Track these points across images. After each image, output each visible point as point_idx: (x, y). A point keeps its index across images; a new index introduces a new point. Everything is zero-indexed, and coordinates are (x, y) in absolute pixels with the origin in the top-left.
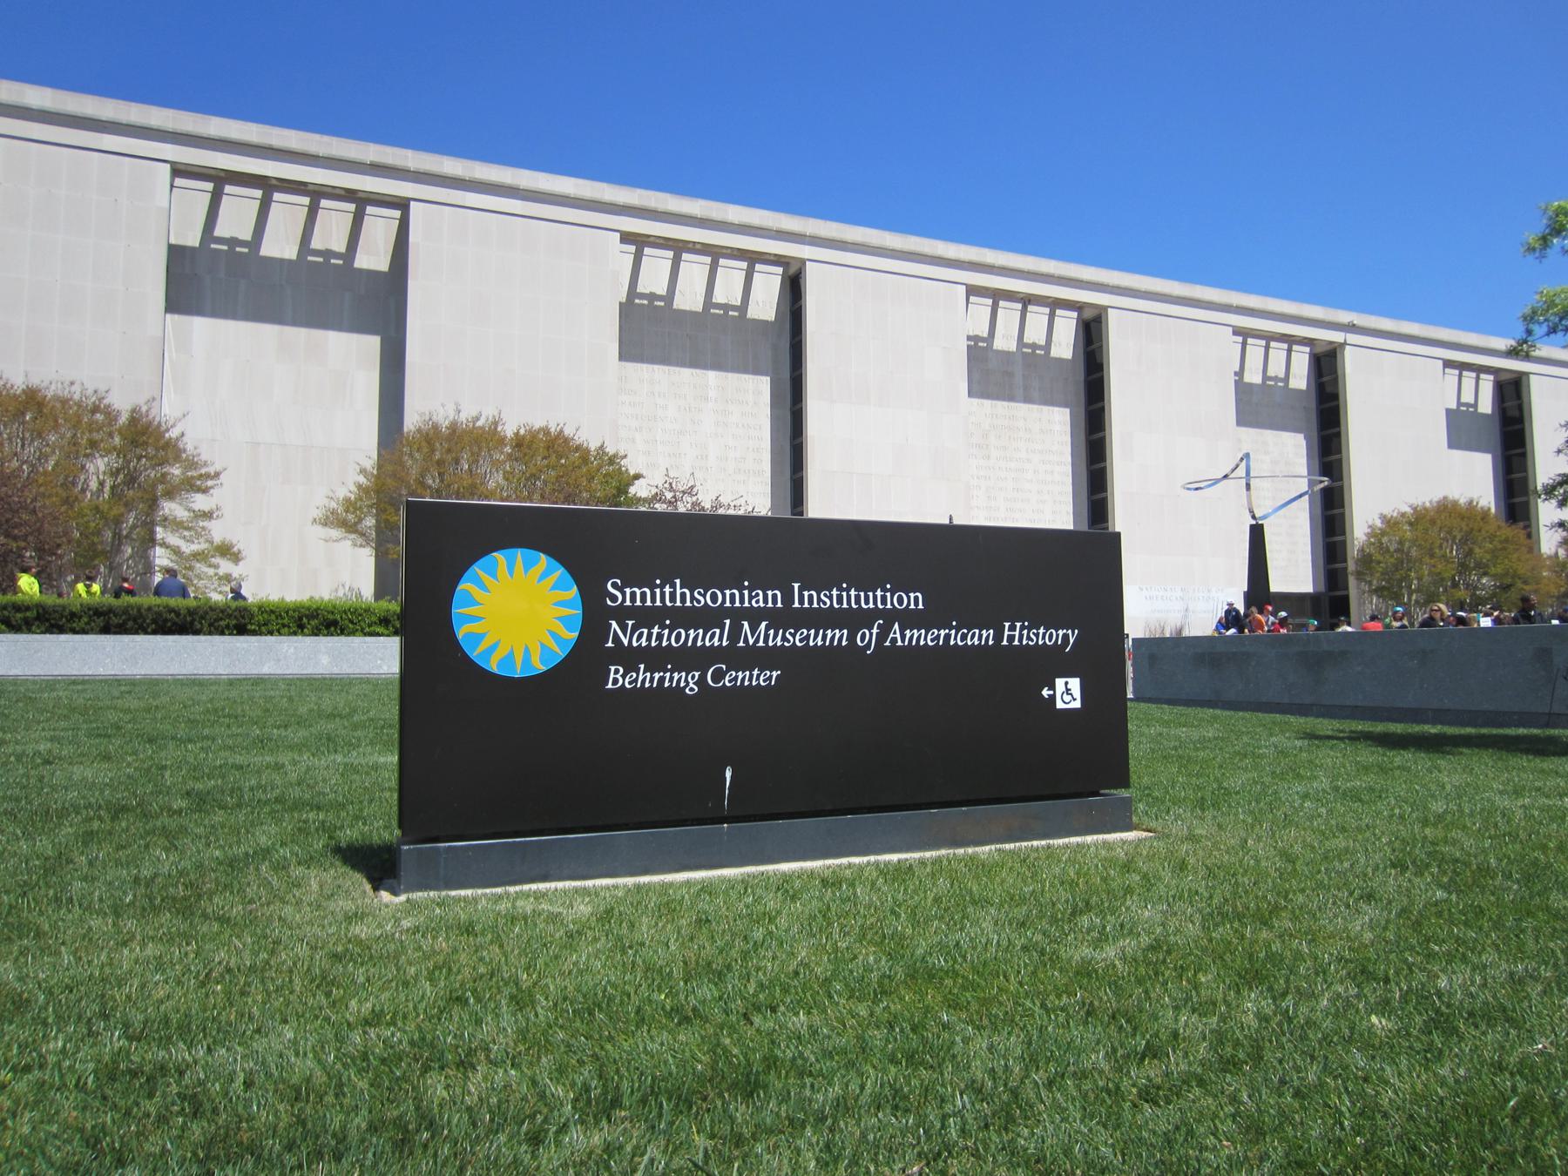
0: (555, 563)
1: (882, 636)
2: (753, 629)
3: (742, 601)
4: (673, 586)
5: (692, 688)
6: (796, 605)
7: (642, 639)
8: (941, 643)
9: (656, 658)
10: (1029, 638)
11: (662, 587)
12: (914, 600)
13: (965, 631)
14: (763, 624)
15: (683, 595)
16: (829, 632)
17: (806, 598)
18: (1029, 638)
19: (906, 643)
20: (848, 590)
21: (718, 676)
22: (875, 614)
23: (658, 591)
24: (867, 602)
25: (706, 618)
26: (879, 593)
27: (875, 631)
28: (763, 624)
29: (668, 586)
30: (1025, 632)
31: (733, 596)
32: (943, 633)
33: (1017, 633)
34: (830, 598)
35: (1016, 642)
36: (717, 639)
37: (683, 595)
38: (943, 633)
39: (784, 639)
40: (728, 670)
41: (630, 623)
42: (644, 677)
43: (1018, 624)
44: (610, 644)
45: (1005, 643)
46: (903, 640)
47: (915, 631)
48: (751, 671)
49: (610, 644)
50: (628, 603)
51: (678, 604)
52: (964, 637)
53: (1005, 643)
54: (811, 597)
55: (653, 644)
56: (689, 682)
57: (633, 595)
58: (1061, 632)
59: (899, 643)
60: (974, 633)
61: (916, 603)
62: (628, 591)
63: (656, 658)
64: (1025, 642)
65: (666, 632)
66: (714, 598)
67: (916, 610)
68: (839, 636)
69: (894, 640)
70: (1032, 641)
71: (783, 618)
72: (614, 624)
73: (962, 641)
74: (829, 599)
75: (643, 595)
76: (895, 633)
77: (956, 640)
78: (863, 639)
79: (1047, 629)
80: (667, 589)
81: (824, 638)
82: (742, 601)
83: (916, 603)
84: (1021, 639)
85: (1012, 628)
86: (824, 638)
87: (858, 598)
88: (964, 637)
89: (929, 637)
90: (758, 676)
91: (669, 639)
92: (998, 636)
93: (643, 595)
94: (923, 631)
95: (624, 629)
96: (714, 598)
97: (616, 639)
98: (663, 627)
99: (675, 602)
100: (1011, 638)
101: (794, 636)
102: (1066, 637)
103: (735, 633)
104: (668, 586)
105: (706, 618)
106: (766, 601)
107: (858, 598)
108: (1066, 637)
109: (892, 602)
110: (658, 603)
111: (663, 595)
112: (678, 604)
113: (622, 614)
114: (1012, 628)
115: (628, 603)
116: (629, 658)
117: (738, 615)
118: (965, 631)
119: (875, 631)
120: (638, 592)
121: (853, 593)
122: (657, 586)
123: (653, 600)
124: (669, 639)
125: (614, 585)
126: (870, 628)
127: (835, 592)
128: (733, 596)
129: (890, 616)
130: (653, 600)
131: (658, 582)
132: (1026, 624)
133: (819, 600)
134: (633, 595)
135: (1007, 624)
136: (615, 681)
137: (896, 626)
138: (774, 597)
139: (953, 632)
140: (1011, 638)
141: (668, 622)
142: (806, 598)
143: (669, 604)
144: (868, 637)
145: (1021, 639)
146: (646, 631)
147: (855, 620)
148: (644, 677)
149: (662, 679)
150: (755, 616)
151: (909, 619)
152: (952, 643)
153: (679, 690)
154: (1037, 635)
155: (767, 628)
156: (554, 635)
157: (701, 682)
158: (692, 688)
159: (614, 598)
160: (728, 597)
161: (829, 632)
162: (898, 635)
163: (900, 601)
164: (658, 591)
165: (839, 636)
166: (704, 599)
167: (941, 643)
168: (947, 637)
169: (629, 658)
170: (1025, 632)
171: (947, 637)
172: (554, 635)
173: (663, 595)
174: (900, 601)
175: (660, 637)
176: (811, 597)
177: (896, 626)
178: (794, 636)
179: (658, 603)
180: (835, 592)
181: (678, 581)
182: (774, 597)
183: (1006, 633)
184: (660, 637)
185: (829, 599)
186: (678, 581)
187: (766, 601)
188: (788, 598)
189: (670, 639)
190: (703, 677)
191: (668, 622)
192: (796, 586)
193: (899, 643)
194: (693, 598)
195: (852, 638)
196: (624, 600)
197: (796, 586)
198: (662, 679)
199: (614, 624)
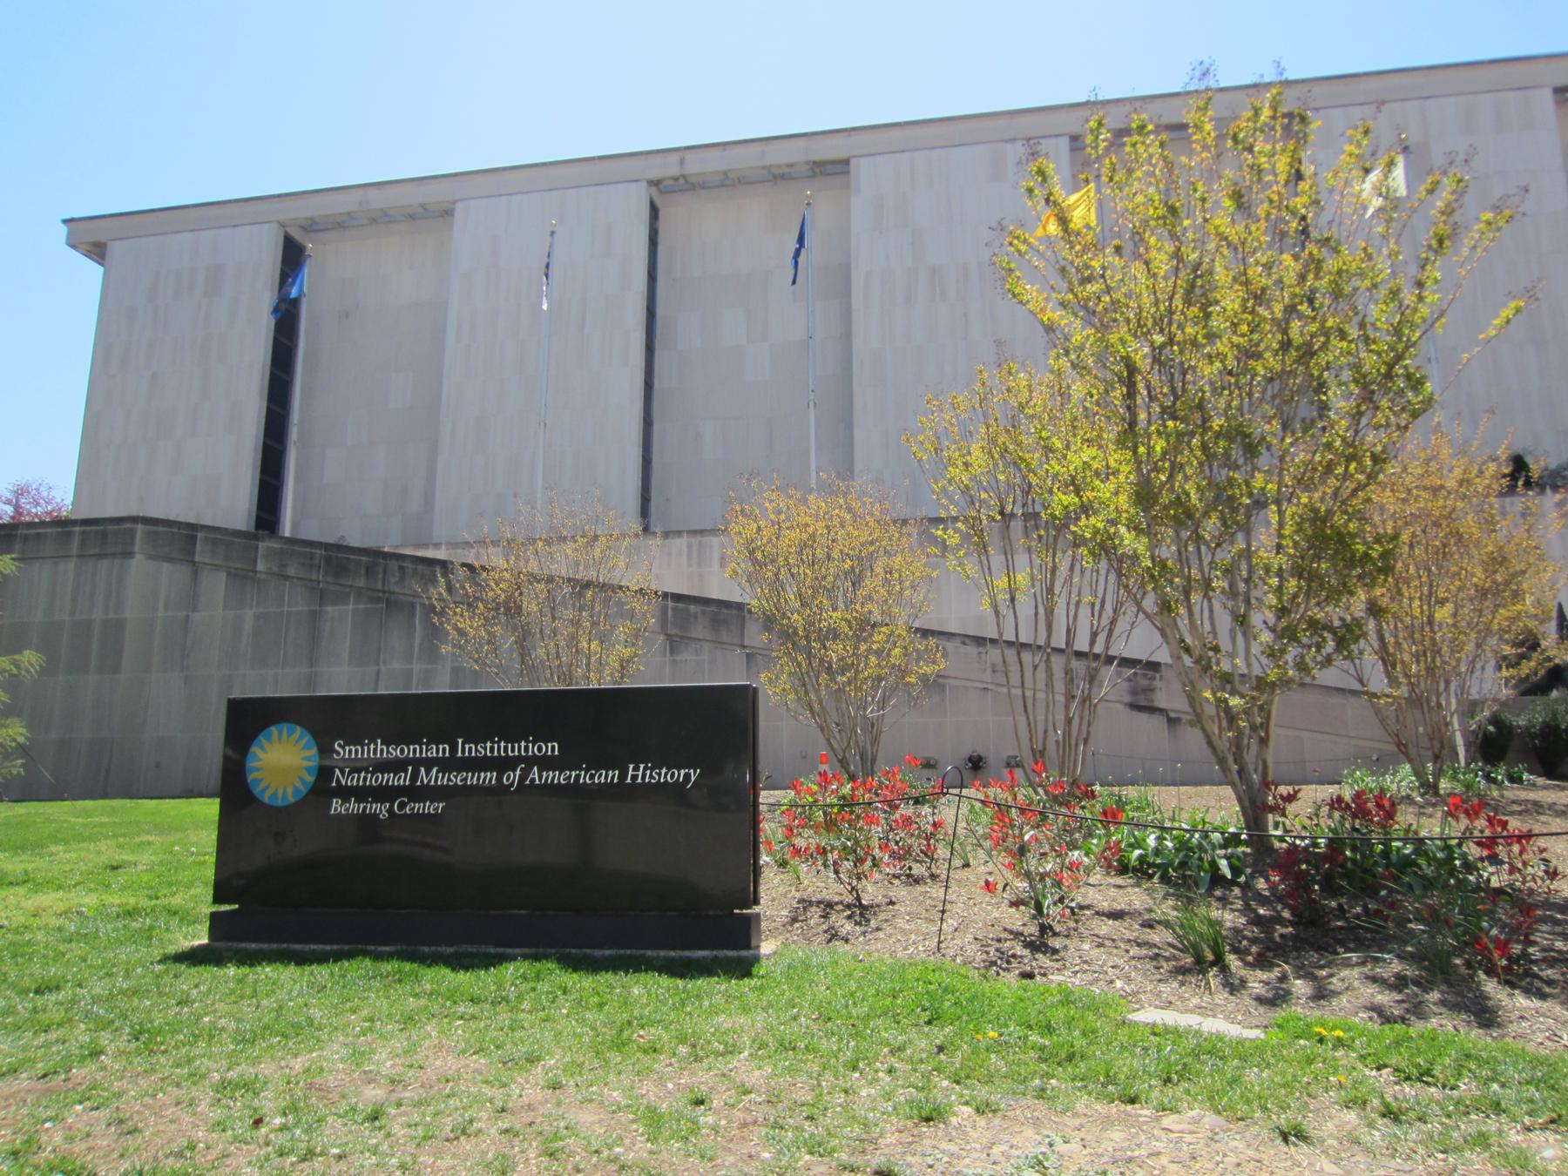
0: (305, 732)
2: (428, 773)
4: (376, 744)
5: (384, 815)
6: (460, 754)
7: (353, 781)
9: (361, 794)
11: (368, 745)
12: (552, 748)
14: (435, 770)
15: (382, 750)
16: (482, 775)
17: (466, 749)
18: (651, 777)
20: (499, 742)
21: (402, 806)
22: (519, 760)
24: (513, 751)
25: (397, 766)
26: (523, 744)
27: (518, 773)
28: (435, 770)
31: (415, 750)
32: (573, 773)
33: (640, 773)
34: (485, 749)
35: (639, 780)
36: (402, 780)
37: (382, 750)
38: (573, 773)
39: (449, 779)
40: (409, 801)
42: (354, 807)
43: (642, 766)
45: (629, 781)
46: (540, 779)
48: (425, 803)
52: (592, 777)
53: (629, 781)
54: (470, 749)
56: (380, 809)
58: (682, 772)
63: (361, 794)
66: (402, 751)
67: (553, 755)
68: (489, 777)
69: (533, 780)
71: (446, 765)
74: (484, 750)
75: (357, 751)
77: (585, 778)
78: (508, 779)
79: (669, 769)
80: (372, 746)
81: (478, 779)
85: (636, 769)
86: (478, 779)
87: (506, 749)
88: (592, 777)
90: (666, 774)
92: (623, 775)
93: (357, 751)
96: (402, 751)
97: (338, 781)
98: (367, 772)
100: (634, 777)
101: (456, 777)
102: (687, 776)
105: (397, 766)
107: (506, 749)
108: (687, 776)
109: (533, 750)
114: (636, 769)
116: (345, 793)
117: (417, 763)
119: (518, 773)
121: (502, 744)
125: (339, 745)
126: (514, 771)
127: (489, 744)
129: (530, 761)
133: (477, 750)
134: (350, 751)
135: (631, 766)
136: (336, 809)
138: (444, 749)
140: (634, 777)
142: (466, 749)
144: (513, 777)
147: (503, 764)
148: (354, 807)
149: (365, 808)
150: (429, 763)
151: (545, 763)
153: (375, 816)
154: (659, 774)
155: (437, 772)
156: (301, 779)
157: (390, 811)
158: (384, 815)
159: (338, 753)
160: (411, 751)
161: (482, 775)
163: (540, 749)
165: (489, 777)
166: (395, 752)
168: (578, 777)
169: (345, 793)
171: (578, 777)
172: (301, 779)
174: (540, 749)
175: (365, 779)
176: (470, 749)
178: (456, 777)
180: (489, 744)
182: (444, 749)
183: (630, 773)
184: (365, 779)
185: (484, 750)
188: (454, 749)
189: (372, 781)
190: (392, 806)
192: (460, 741)
193: (537, 782)
194: (388, 752)
195: (499, 779)
197: (460, 741)
198: (365, 808)
199: (337, 771)
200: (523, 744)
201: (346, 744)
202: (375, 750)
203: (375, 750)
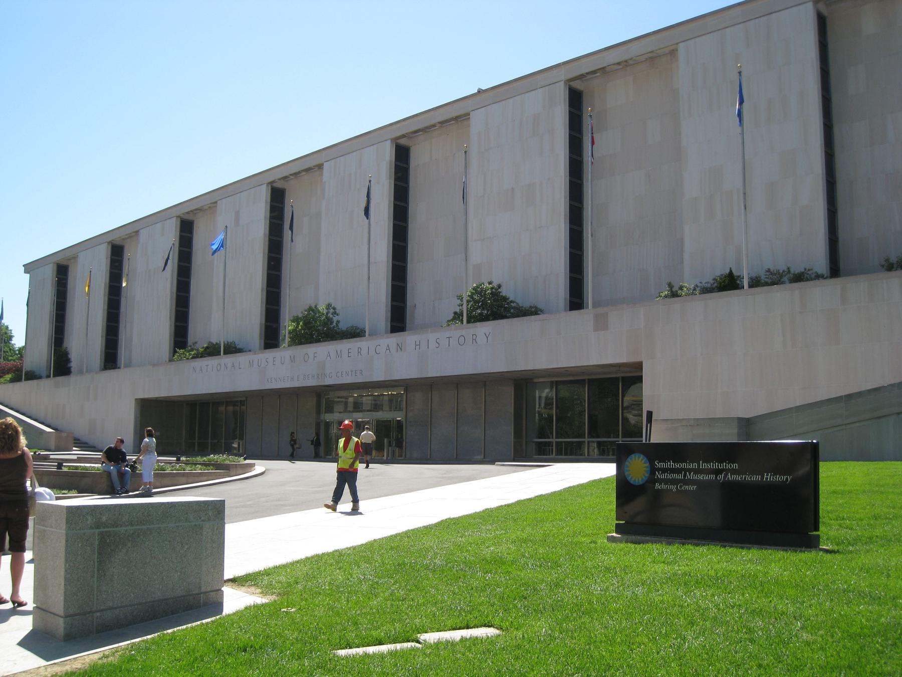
1: (725, 477)
2: (690, 474)
3: (687, 466)
7: (662, 476)
9: (666, 481)
14: (692, 473)
15: (672, 465)
24: (721, 467)
25: (678, 471)
28: (692, 473)
31: (684, 465)
36: (681, 477)
37: (672, 465)
46: (731, 478)
52: (751, 478)
57: (661, 465)
61: (695, 467)
63: (666, 481)
66: (680, 465)
79: (780, 476)
82: (687, 466)
83: (695, 467)
85: (767, 475)
87: (718, 465)
88: (751, 478)
96: (680, 465)
100: (767, 478)
102: (787, 479)
103: (685, 475)
105: (678, 471)
106: (693, 466)
107: (718, 465)
108: (787, 479)
109: (728, 466)
113: (659, 470)
114: (767, 475)
116: (661, 481)
117: (686, 470)
121: (717, 464)
128: (684, 465)
129: (727, 471)
134: (661, 465)
138: (695, 465)
140: (767, 478)
144: (721, 477)
150: (690, 470)
151: (733, 472)
156: (644, 475)
160: (683, 465)
168: (745, 478)
169: (661, 481)
171: (745, 478)
174: (731, 466)
175: (667, 476)
176: (705, 465)
182: (695, 465)
184: (667, 476)
187: (693, 466)
188: (699, 465)
189: (669, 477)
195: (716, 477)
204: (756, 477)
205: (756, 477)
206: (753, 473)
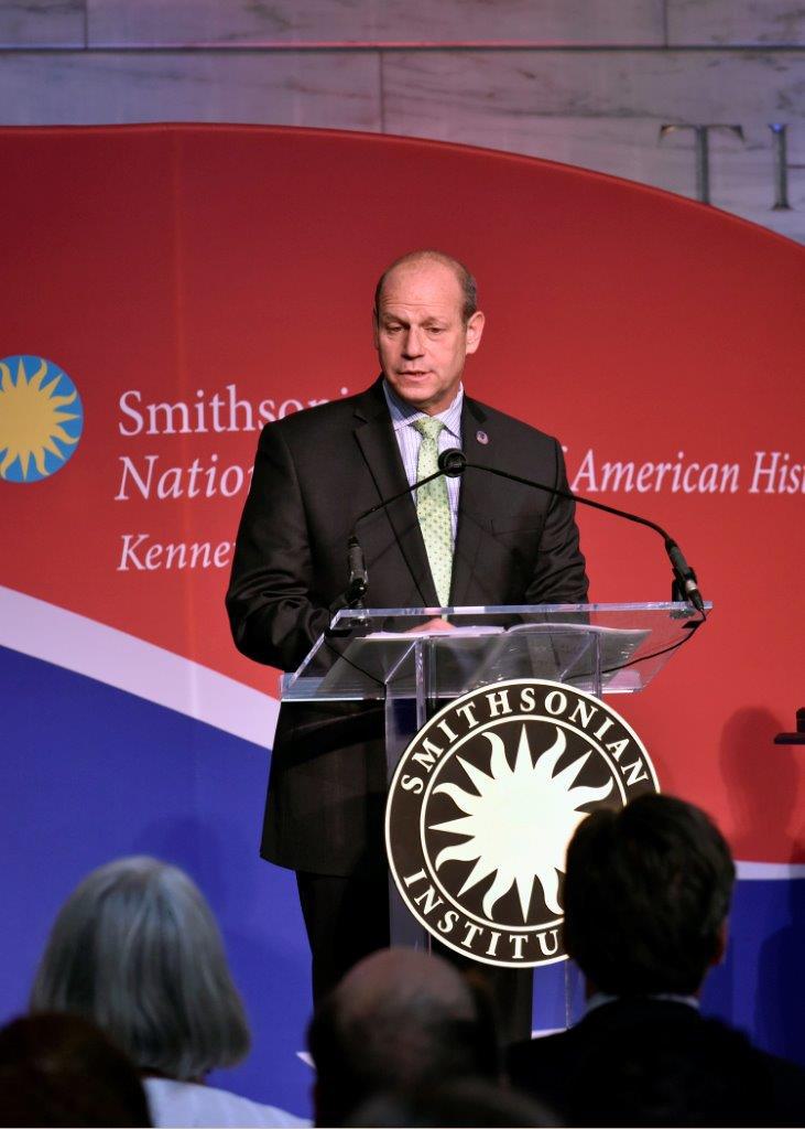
4: (225, 397)
8: (658, 488)
10: (789, 482)
11: (207, 400)
13: (696, 466)
15: (241, 412)
19: (604, 487)
23: (200, 407)
29: (216, 398)
30: (784, 469)
33: (772, 472)
35: (770, 489)
37: (241, 412)
38: (662, 469)
41: (152, 459)
43: (776, 456)
44: (122, 496)
45: (754, 489)
46: (599, 482)
47: (619, 466)
49: (122, 496)
50: (153, 430)
51: (233, 427)
52: (694, 479)
53: (754, 489)
55: (192, 493)
57: (161, 415)
59: (593, 488)
60: (710, 471)
62: (152, 409)
64: (781, 489)
65: (212, 471)
70: (793, 486)
72: (128, 462)
73: (690, 485)
75: (177, 414)
76: (586, 470)
80: (216, 403)
84: (776, 485)
85: (767, 463)
88: (694, 479)
89: (640, 478)
91: (217, 485)
92: (745, 479)
93: (177, 414)
94: (631, 466)
95: (142, 468)
97: (132, 488)
99: (228, 425)
100: (764, 479)
104: (216, 398)
110: (201, 428)
111: (208, 412)
112: (233, 427)
113: (139, 447)
114: (767, 463)
115: (153, 430)
118: (696, 466)
120: (169, 410)
122: (199, 400)
123: (193, 422)
124: (217, 485)
125: (131, 402)
130: (193, 422)
131: (200, 393)
132: (787, 457)
134: (161, 415)
137: (590, 457)
139: (678, 468)
140: (764, 479)
141: (214, 458)
143: (218, 428)
145: (776, 485)
146: (178, 471)
152: (675, 488)
159: (131, 424)
162: (591, 475)
164: (200, 407)
167: (658, 488)
168: (669, 476)
170: (784, 469)
171: (669, 476)
173: (208, 412)
175: (202, 481)
177: (590, 457)
179: (201, 428)
181: (232, 389)
183: (758, 471)
184: (202, 481)
186: (232, 389)
191: (214, 458)
193: (593, 488)
194: (257, 416)
196: (147, 426)
200: (195, 470)
201: (147, 400)
202: (224, 412)
203: (224, 412)
204: (720, 475)
205: (720, 475)
206: (702, 454)
